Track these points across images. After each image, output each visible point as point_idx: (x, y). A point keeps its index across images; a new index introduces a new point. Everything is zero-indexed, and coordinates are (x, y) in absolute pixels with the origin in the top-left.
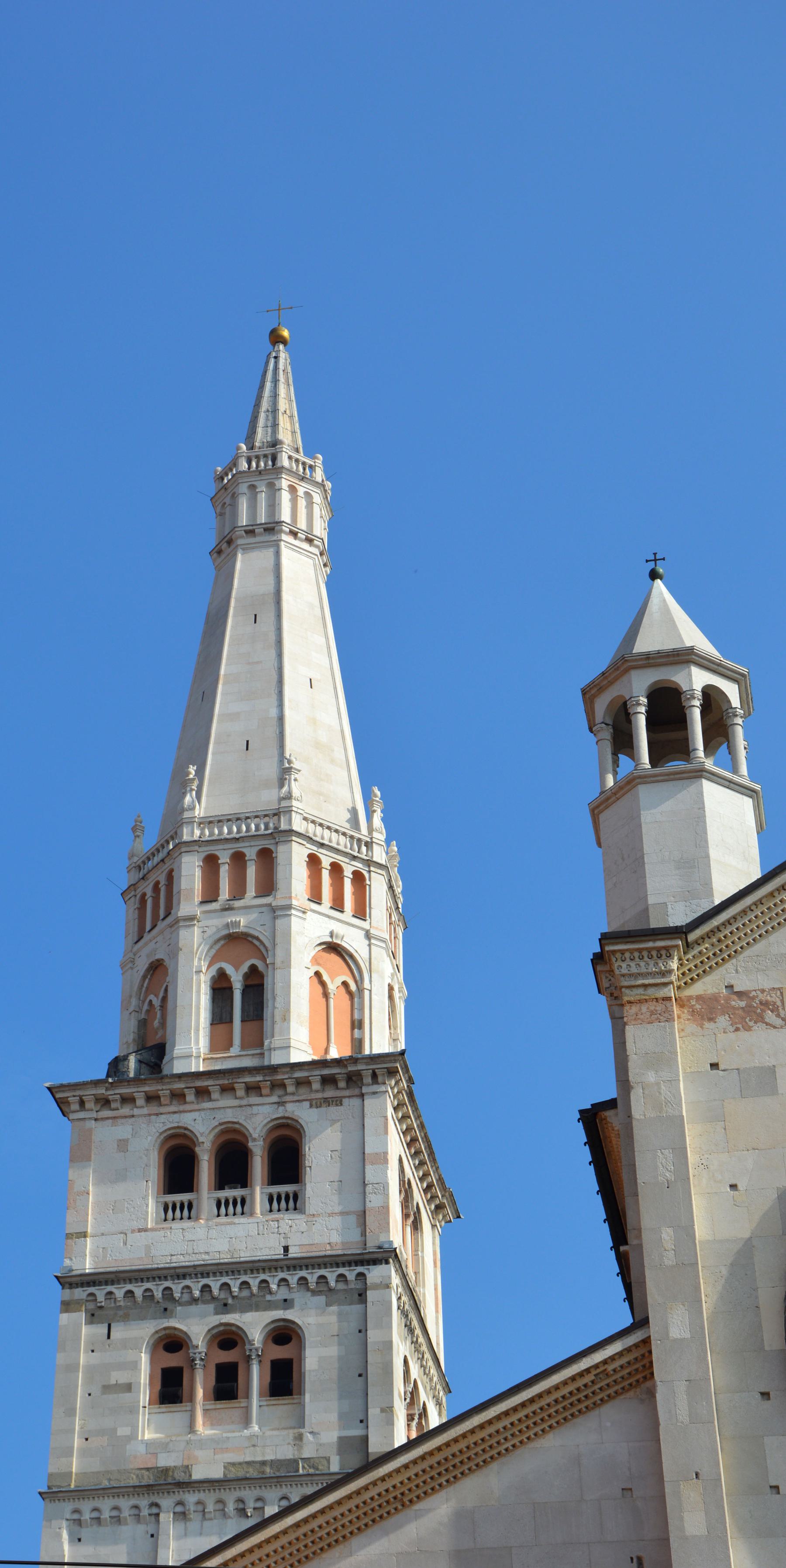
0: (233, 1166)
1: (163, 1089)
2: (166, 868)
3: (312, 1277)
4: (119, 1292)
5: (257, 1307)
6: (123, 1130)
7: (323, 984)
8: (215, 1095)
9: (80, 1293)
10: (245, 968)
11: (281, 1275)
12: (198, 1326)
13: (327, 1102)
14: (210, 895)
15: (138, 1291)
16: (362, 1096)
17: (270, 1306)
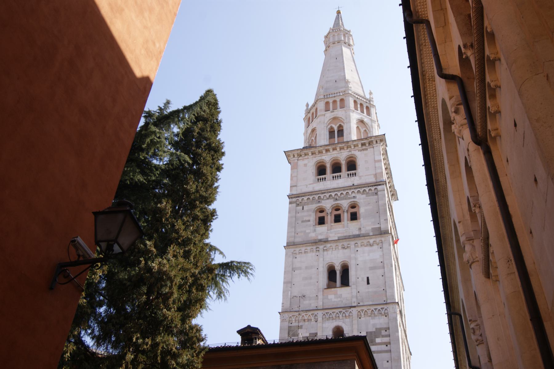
0: (337, 168)
1: (317, 150)
2: (315, 108)
3: (362, 190)
4: (305, 198)
5: (346, 199)
6: (306, 162)
7: (359, 129)
8: (331, 151)
9: (294, 200)
10: (338, 125)
11: (352, 190)
12: (328, 205)
13: (363, 150)
14: (327, 110)
15: (311, 198)
16: (373, 147)
17: (350, 198)
